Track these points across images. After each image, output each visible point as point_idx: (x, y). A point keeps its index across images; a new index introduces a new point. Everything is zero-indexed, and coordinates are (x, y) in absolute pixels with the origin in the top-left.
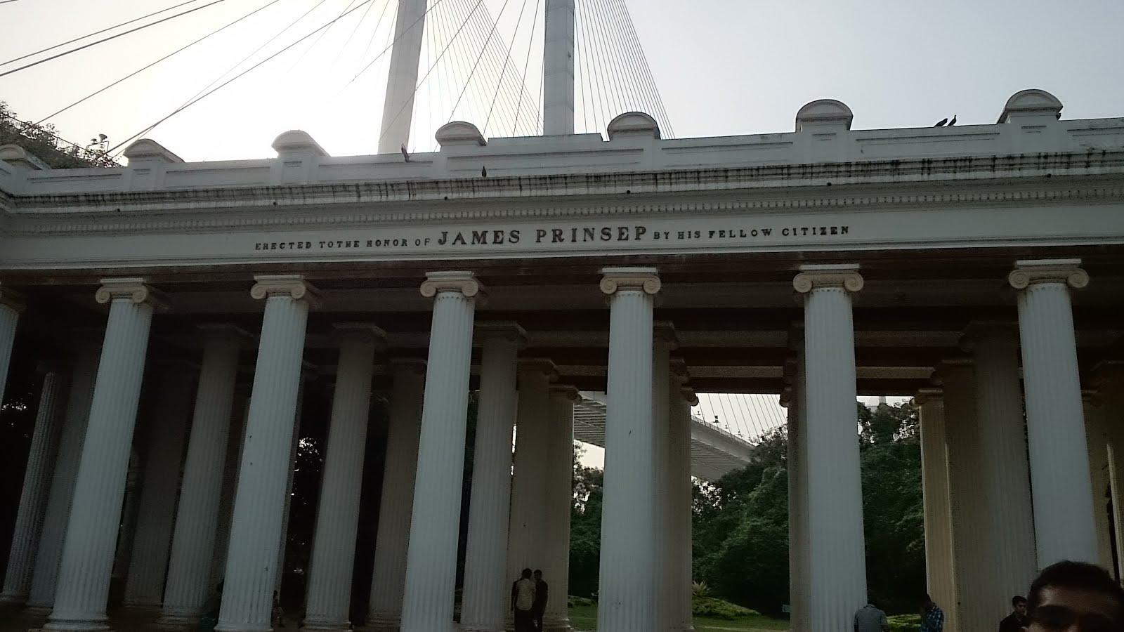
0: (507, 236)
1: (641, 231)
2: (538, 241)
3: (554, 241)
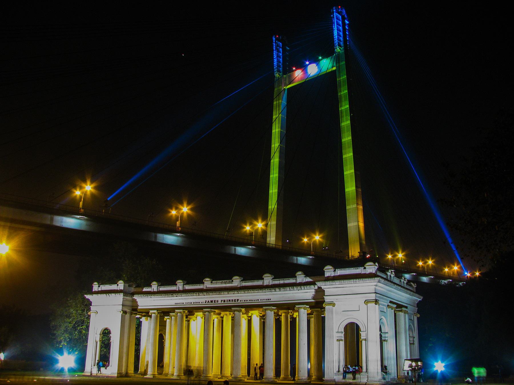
0: (216, 301)
1: (238, 300)
2: (221, 302)
3: (224, 302)
